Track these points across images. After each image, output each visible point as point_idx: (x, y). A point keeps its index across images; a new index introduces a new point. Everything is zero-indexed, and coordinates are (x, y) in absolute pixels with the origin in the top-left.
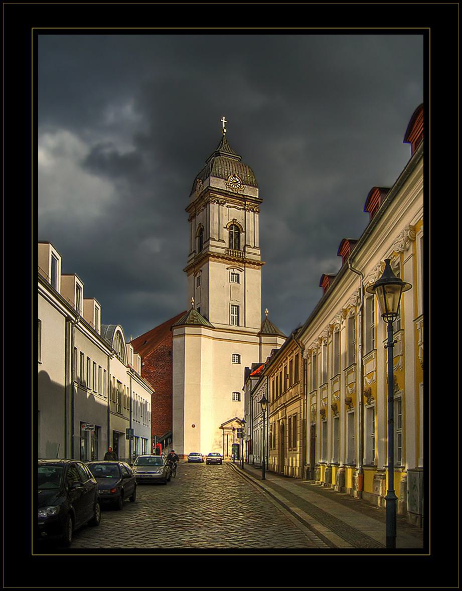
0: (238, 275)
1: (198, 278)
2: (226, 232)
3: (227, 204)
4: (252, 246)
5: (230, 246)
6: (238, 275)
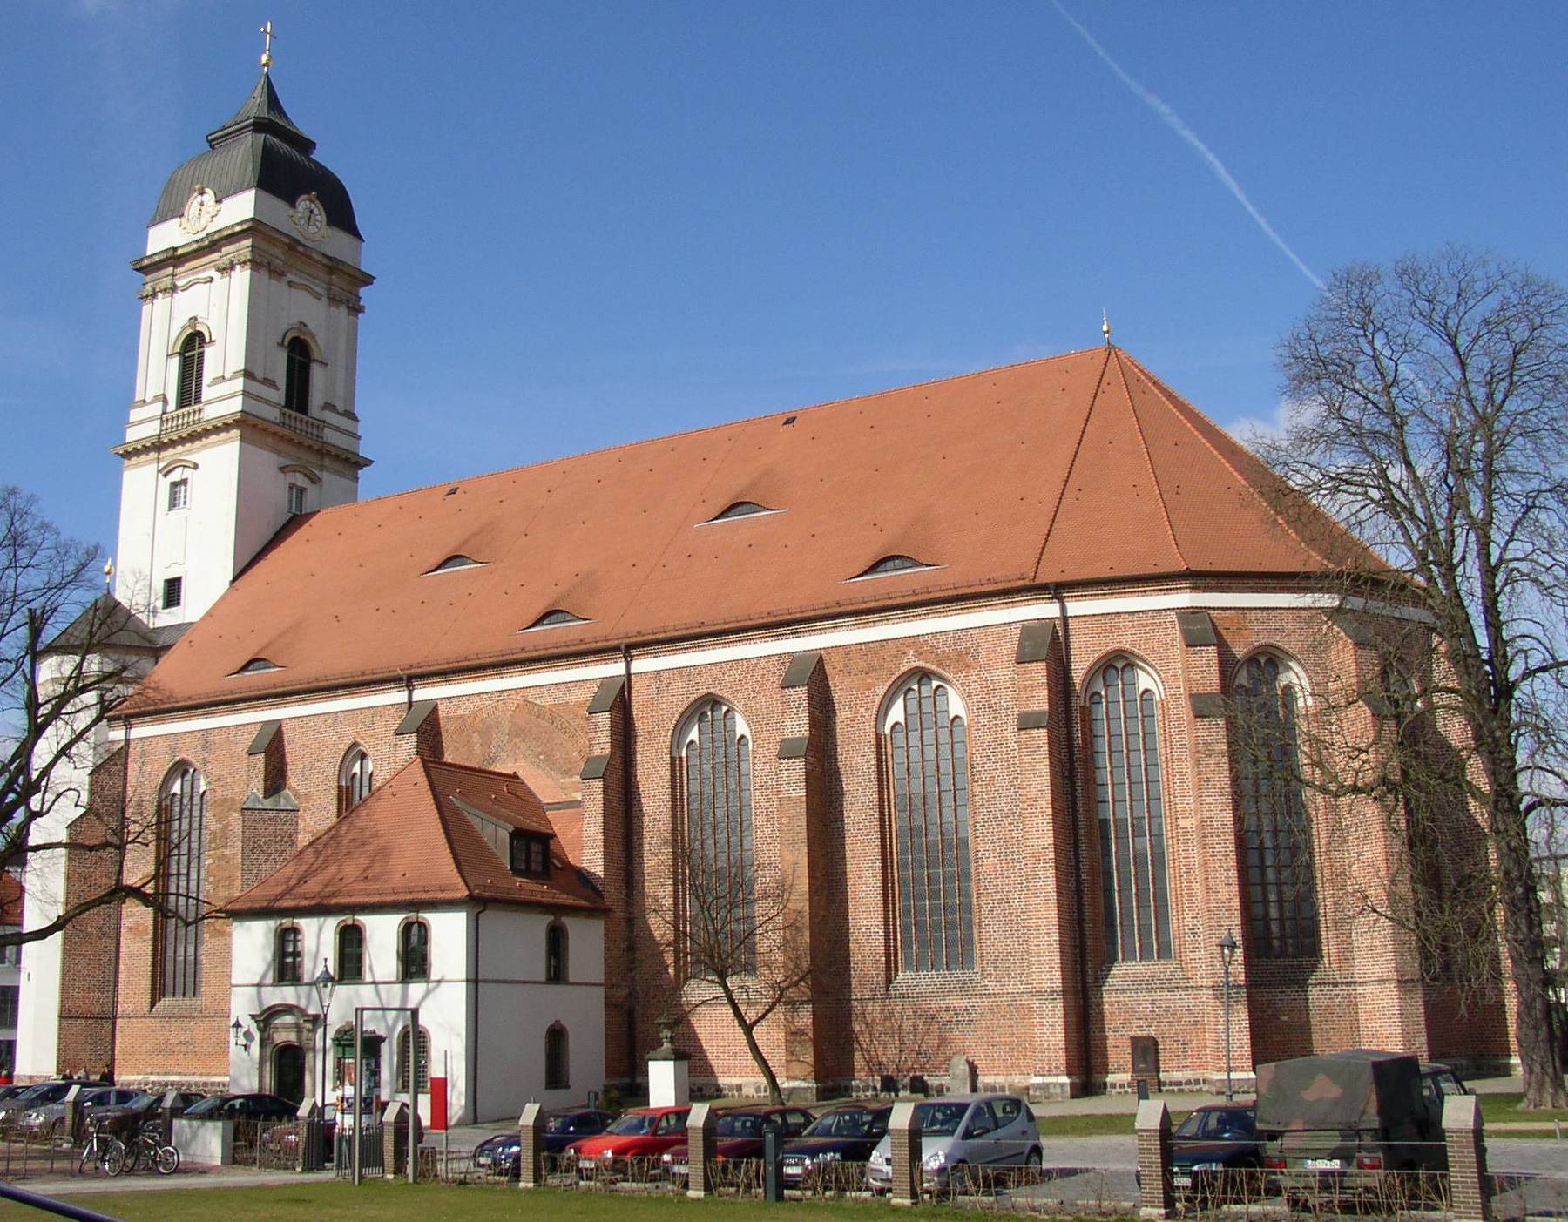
0: (301, 491)
1: (174, 485)
2: (282, 357)
3: (290, 277)
4: (341, 408)
5: (288, 404)
6: (301, 491)
